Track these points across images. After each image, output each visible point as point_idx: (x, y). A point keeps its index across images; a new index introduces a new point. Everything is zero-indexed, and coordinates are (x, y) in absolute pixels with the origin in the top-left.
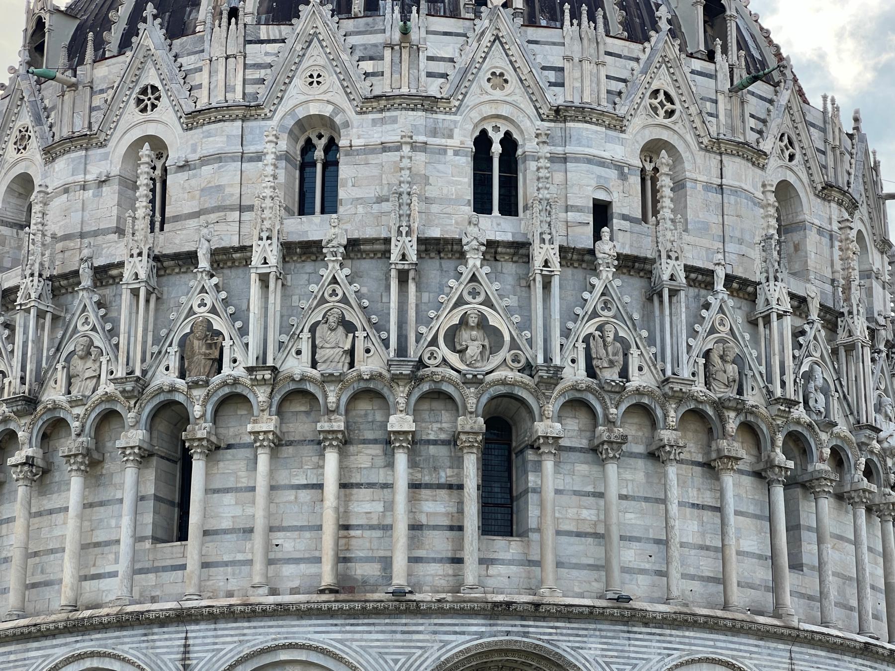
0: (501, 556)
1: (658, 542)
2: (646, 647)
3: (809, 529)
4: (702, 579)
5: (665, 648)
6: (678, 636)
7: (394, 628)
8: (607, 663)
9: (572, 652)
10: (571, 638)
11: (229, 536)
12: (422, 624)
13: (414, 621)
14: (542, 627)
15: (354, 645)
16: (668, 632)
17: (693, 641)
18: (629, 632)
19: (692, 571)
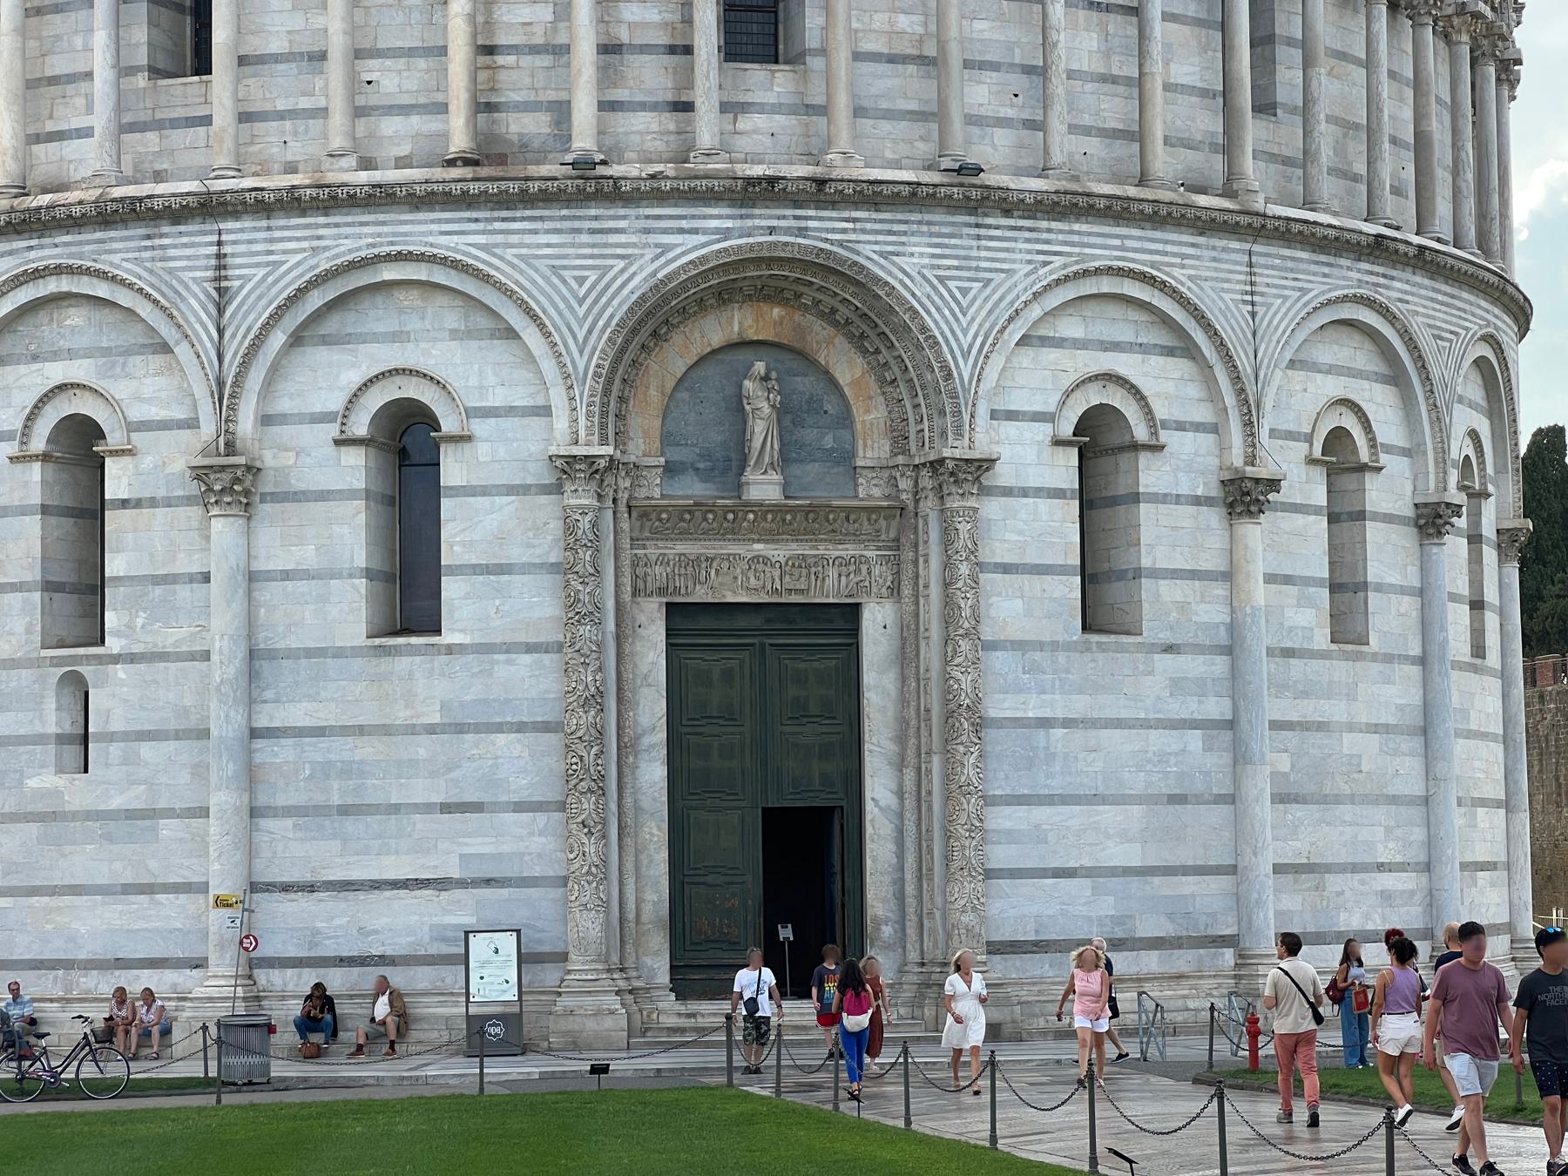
0: (757, 97)
1: (1029, 70)
2: (1007, 250)
3: (1290, 42)
4: (1104, 133)
5: (1039, 252)
6: (1061, 232)
7: (577, 224)
8: (941, 279)
9: (882, 261)
10: (880, 238)
11: (282, 67)
12: (624, 217)
13: (611, 212)
14: (831, 219)
15: (509, 253)
16: (1044, 224)
17: (1086, 239)
18: (977, 226)
19: (1087, 120)
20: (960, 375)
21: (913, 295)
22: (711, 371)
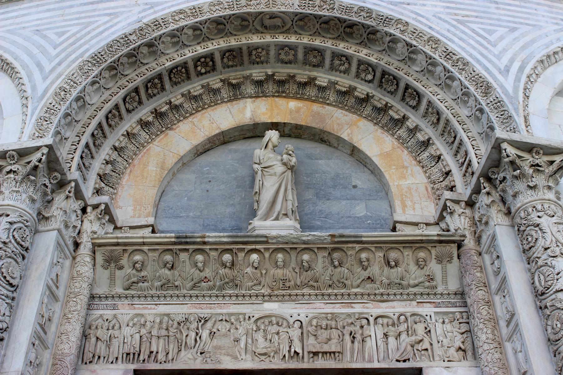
20: (502, 87)
21: (430, 28)
22: (224, 157)
